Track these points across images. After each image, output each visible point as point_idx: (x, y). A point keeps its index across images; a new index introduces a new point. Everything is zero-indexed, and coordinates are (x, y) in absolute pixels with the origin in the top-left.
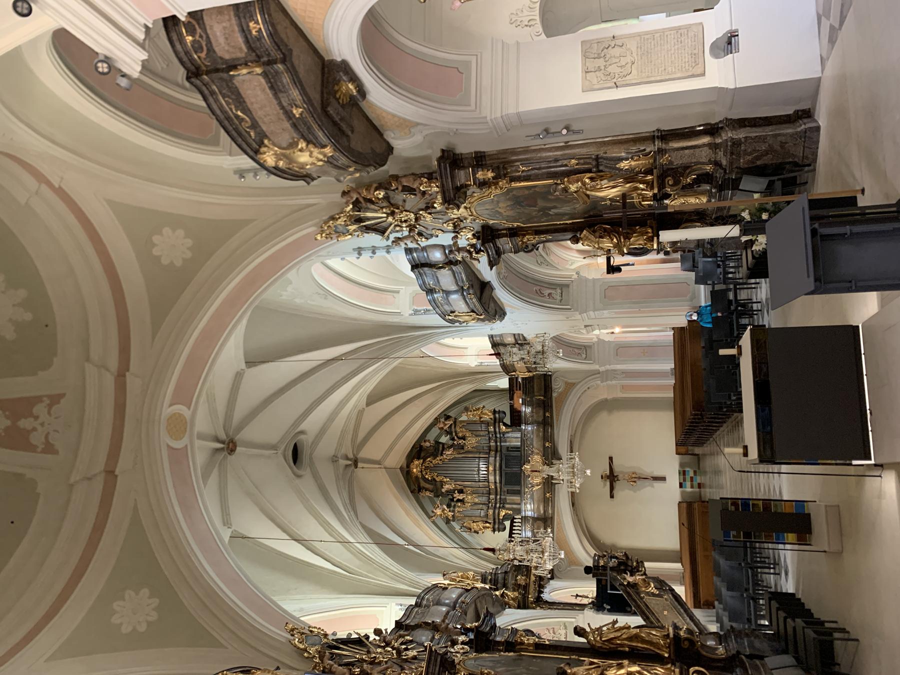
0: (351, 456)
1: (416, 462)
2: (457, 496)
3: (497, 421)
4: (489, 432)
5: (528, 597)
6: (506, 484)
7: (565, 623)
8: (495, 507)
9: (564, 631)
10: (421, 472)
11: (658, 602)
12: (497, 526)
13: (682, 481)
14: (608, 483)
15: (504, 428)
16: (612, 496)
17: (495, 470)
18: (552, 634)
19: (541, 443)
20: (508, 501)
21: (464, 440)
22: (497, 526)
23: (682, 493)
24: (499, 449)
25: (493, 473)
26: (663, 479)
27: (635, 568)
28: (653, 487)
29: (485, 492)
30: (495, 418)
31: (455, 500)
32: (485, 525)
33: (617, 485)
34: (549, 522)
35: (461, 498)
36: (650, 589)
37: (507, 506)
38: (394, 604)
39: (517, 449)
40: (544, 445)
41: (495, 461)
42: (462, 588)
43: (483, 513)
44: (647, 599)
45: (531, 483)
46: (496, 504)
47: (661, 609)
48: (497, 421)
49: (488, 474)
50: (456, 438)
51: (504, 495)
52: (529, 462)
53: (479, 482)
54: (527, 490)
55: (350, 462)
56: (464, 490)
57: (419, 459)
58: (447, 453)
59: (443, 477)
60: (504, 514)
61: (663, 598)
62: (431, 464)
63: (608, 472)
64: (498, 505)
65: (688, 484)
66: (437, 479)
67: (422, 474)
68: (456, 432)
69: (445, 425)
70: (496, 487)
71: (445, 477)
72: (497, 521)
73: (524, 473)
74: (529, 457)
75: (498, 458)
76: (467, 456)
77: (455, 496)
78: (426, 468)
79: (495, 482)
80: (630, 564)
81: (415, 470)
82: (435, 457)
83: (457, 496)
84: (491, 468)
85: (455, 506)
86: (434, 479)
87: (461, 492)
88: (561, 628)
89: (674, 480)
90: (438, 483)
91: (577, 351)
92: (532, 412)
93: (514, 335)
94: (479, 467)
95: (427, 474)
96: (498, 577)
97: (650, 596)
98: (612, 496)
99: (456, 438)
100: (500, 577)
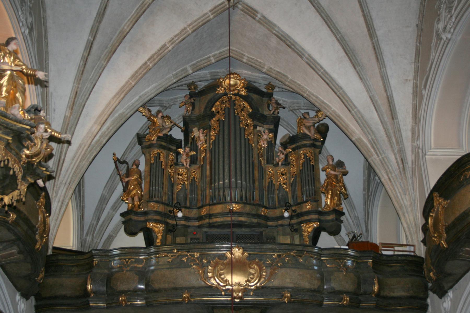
3: (323, 218)
10: (226, 94)
15: (310, 230)
22: (135, 218)
24: (270, 223)
30: (328, 213)
41: (248, 215)
48: (323, 218)
54: (197, 255)
56: (196, 166)
64: (170, 221)
66: (213, 122)
68: (299, 148)
69: (308, 128)
71: (219, 131)
72: (142, 218)
74: (260, 260)
75: (255, 220)
76: (256, 168)
79: (210, 216)
86: (213, 115)
87: (193, 160)
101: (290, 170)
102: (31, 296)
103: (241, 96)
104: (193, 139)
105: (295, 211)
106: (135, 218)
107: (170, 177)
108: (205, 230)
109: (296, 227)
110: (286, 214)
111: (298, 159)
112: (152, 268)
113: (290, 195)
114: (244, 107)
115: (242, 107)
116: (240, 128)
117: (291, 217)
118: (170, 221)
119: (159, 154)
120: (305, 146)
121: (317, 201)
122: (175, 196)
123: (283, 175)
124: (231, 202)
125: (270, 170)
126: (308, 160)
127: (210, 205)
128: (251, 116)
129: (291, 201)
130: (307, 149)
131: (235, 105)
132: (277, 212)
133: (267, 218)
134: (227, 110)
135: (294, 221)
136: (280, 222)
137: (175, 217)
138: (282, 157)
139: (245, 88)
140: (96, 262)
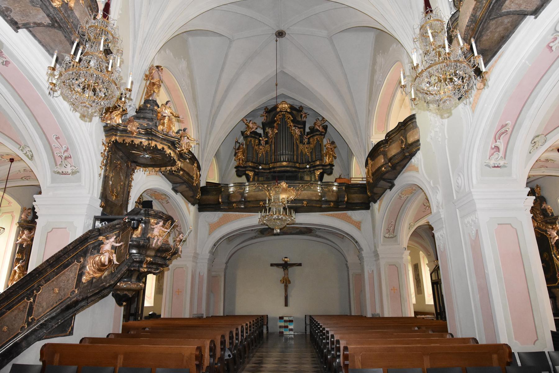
3: (324, 168)
4: (314, 161)
5: (116, 135)
7: (78, 172)
9: (70, 171)
11: (70, 281)
15: (319, 173)
16: (272, 265)
21: (307, 144)
22: (240, 169)
23: (274, 319)
24: (301, 170)
26: (286, 305)
30: (327, 166)
32: (241, 160)
35: (262, 142)
39: (302, 179)
40: (304, 200)
41: (291, 167)
44: (75, 267)
45: (271, 189)
47: (62, 284)
48: (324, 168)
50: (309, 136)
54: (266, 186)
60: (250, 174)
61: (76, 288)
62: (287, 119)
64: (256, 170)
65: (283, 324)
67: (279, 112)
68: (314, 136)
69: (319, 126)
72: (244, 169)
74: (293, 188)
75: (294, 169)
76: (295, 145)
79: (274, 168)
84: (285, 164)
86: (276, 122)
89: (283, 311)
91: (392, 228)
92: (333, 191)
93: (418, 141)
95: (280, 116)
97: (80, 270)
98: (272, 265)
99: (309, 136)
101: (310, 146)
102: (196, 204)
103: (288, 112)
104: (266, 133)
105: (312, 165)
106: (240, 169)
107: (256, 150)
108: (272, 174)
109: (312, 172)
110: (308, 166)
111: (314, 141)
112: (247, 192)
113: (310, 158)
114: (290, 117)
116: (288, 127)
117: (310, 168)
118: (256, 170)
119: (251, 140)
120: (317, 135)
121: (321, 159)
122: (259, 159)
123: (307, 148)
124: (283, 161)
125: (301, 146)
126: (318, 141)
127: (274, 163)
128: (292, 121)
129: (310, 160)
130: (317, 137)
131: (285, 116)
132: (304, 165)
133: (299, 168)
134: (282, 119)
135: (312, 169)
136: (305, 170)
137: (258, 169)
138: (306, 140)
139: (290, 109)
140: (223, 190)
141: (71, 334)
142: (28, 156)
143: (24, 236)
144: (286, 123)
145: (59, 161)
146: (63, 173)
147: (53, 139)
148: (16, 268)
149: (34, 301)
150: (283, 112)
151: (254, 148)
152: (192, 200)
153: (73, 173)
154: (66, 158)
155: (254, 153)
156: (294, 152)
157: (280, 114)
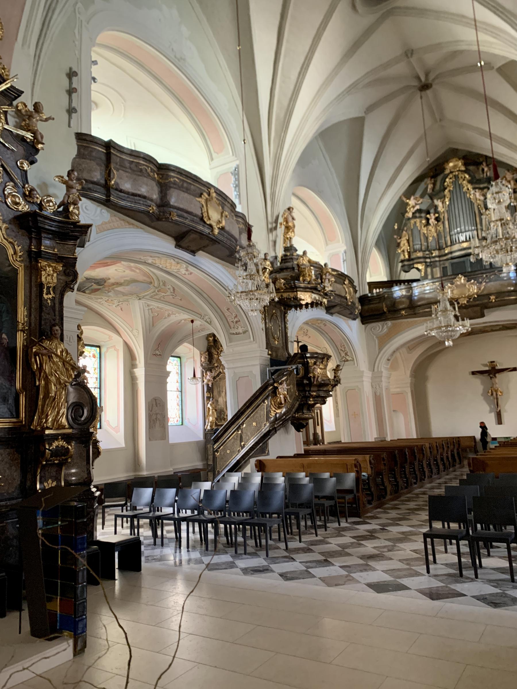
0: (431, 77)
1: (460, 163)
2: (432, 218)
6: (452, 264)
8: (426, 258)
9: (241, 332)
10: (451, 172)
11: (262, 417)
12: (406, 263)
13: (498, 440)
14: (487, 369)
16: (473, 373)
17: (465, 249)
18: (235, 320)
19: (493, 290)
20: (434, 270)
22: (406, 263)
25: (460, 248)
27: (309, 394)
28: (490, 412)
29: (441, 245)
31: (428, 216)
32: (406, 251)
33: (485, 377)
34: (411, 312)
35: (430, 221)
36: (274, 409)
37: (429, 270)
38: (237, 162)
40: (491, 294)
42: (202, 214)
43: (418, 247)
46: (429, 258)
49: (459, 243)
51: (440, 265)
52: (468, 281)
53: (450, 236)
55: (423, 79)
57: (465, 164)
58: (478, 194)
59: (449, 197)
63: (499, 367)
64: (428, 260)
70: (446, 255)
73: (455, 278)
77: (432, 215)
78: (456, 177)
79: (451, 253)
80: (312, 389)
81: (451, 164)
82: (470, 182)
83: (432, 218)
85: (421, 217)
86: (446, 189)
87: (437, 219)
88: (243, 328)
90: (442, 193)
94: (466, 231)
95: (450, 178)
96: (289, 262)
98: (473, 373)
100: (289, 264)
103: (462, 171)
108: (450, 261)
114: (465, 177)
115: (463, 177)
116: (464, 193)
119: (415, 222)
122: (429, 245)
124: (463, 242)
141: (268, 454)
142: (208, 322)
143: (208, 377)
144: (461, 186)
145: (232, 325)
146: (237, 334)
147: (224, 309)
148: (209, 406)
149: (242, 432)
150: (455, 172)
151: (422, 232)
152: (352, 316)
153: (244, 332)
154: (236, 322)
155: (422, 238)
156: (477, 226)
157: (451, 176)
